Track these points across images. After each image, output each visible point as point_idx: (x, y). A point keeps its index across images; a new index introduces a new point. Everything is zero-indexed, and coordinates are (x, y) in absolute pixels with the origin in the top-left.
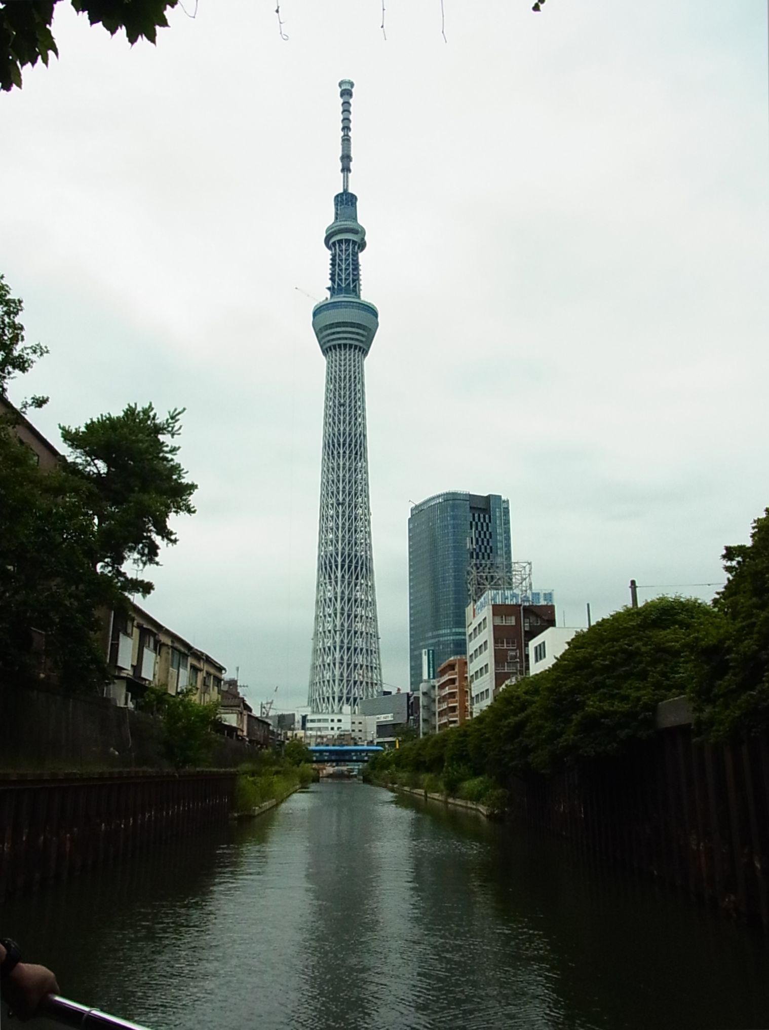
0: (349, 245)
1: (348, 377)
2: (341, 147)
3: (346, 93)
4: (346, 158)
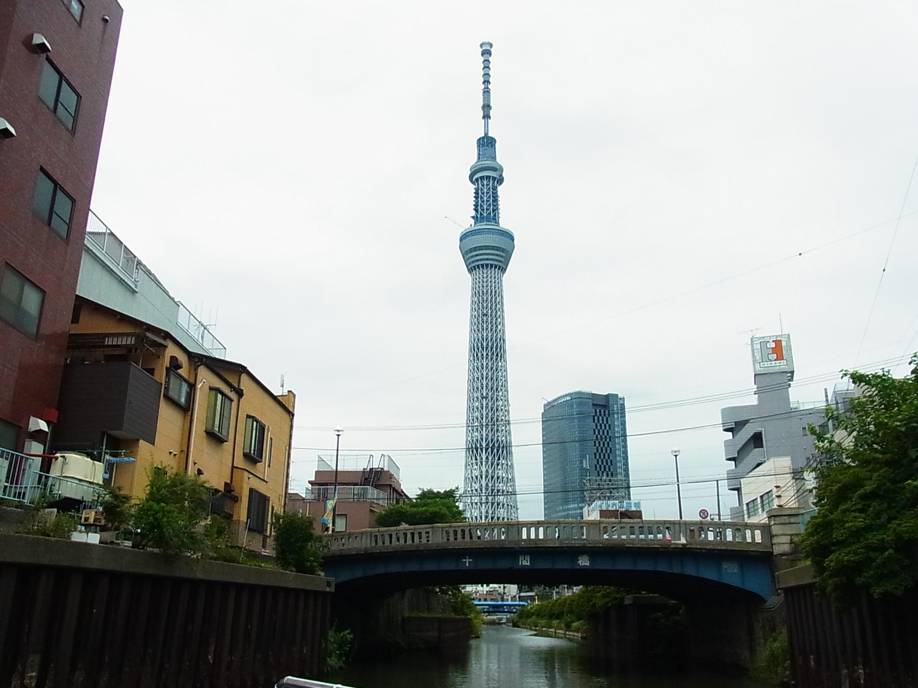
0: (489, 180)
1: (489, 291)
2: (482, 97)
3: (486, 53)
4: (487, 107)
